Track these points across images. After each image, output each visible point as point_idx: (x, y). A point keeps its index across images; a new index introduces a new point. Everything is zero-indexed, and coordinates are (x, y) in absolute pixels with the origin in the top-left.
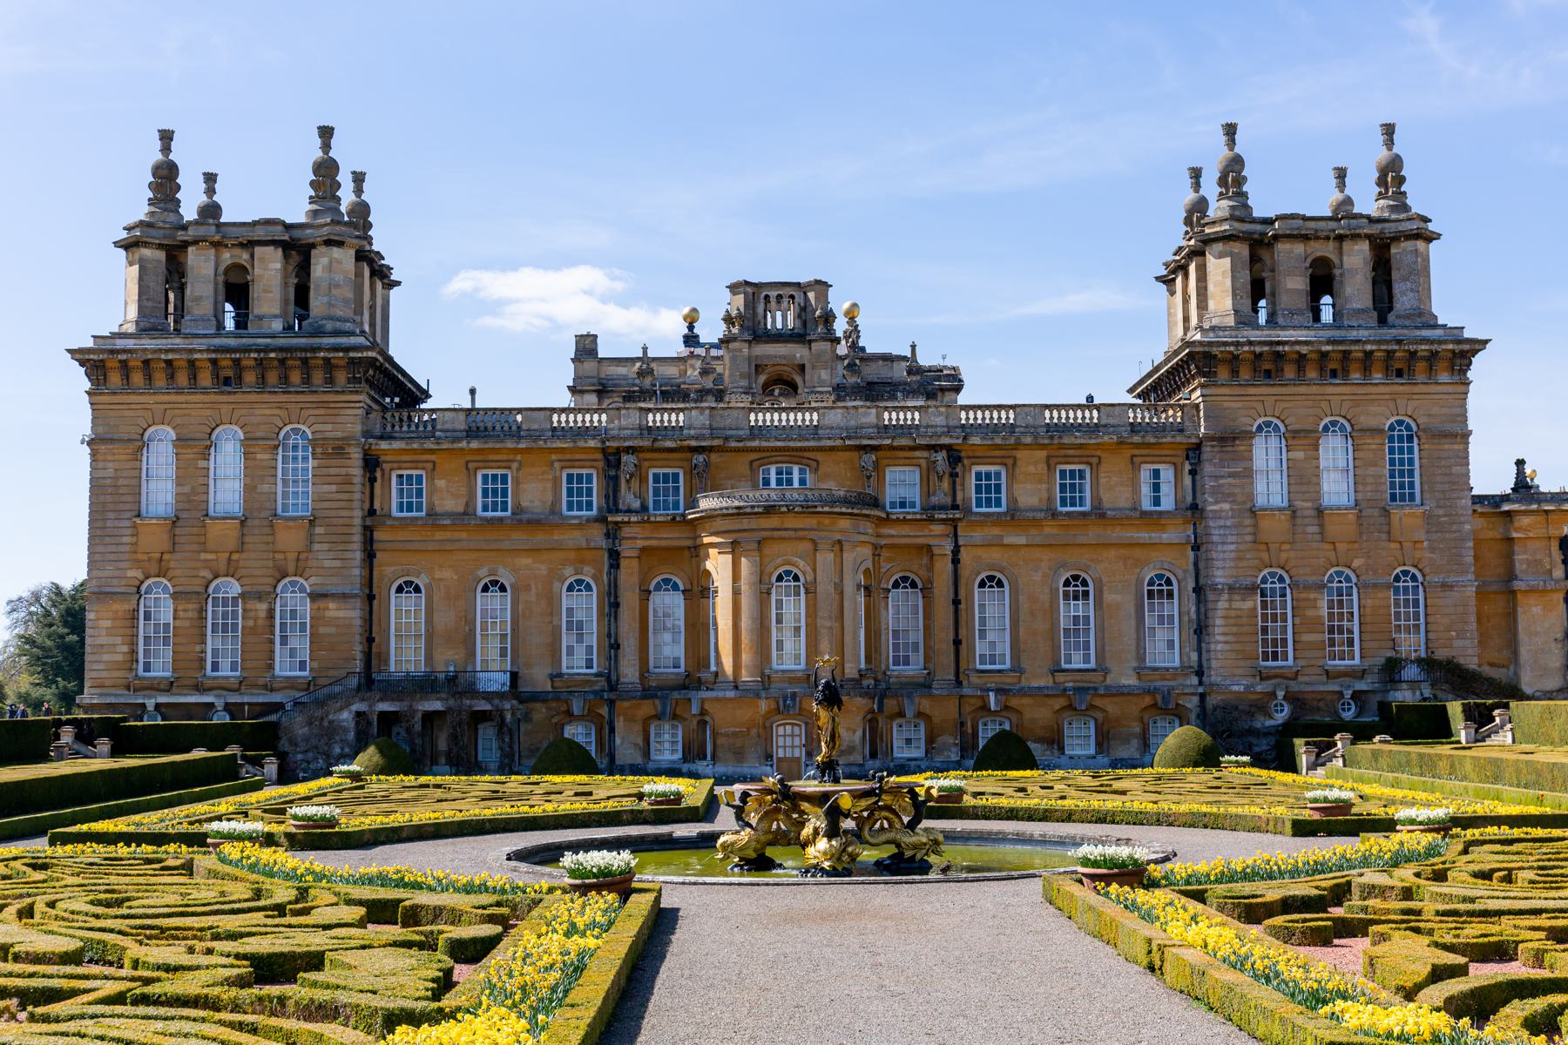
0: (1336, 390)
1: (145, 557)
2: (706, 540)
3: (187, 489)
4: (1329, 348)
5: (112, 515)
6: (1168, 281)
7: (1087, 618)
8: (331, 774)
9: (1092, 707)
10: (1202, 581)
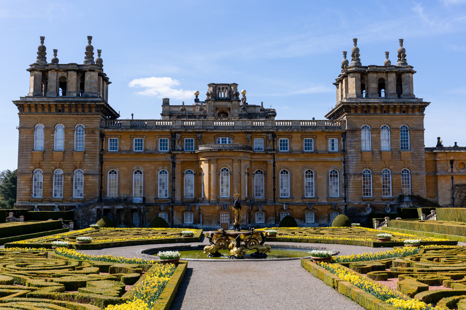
0: (386, 117)
1: (35, 162)
2: (201, 159)
3: (47, 143)
4: (384, 104)
5: (25, 150)
6: (336, 85)
7: (312, 183)
8: (89, 227)
9: (314, 209)
10: (346, 172)
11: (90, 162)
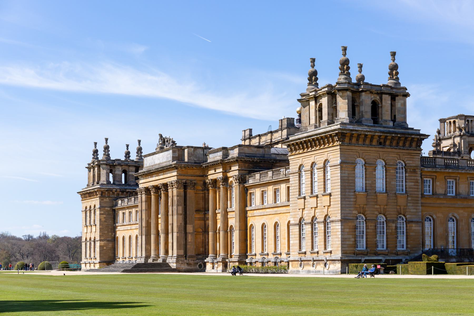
5: (347, 190)
11: (413, 208)
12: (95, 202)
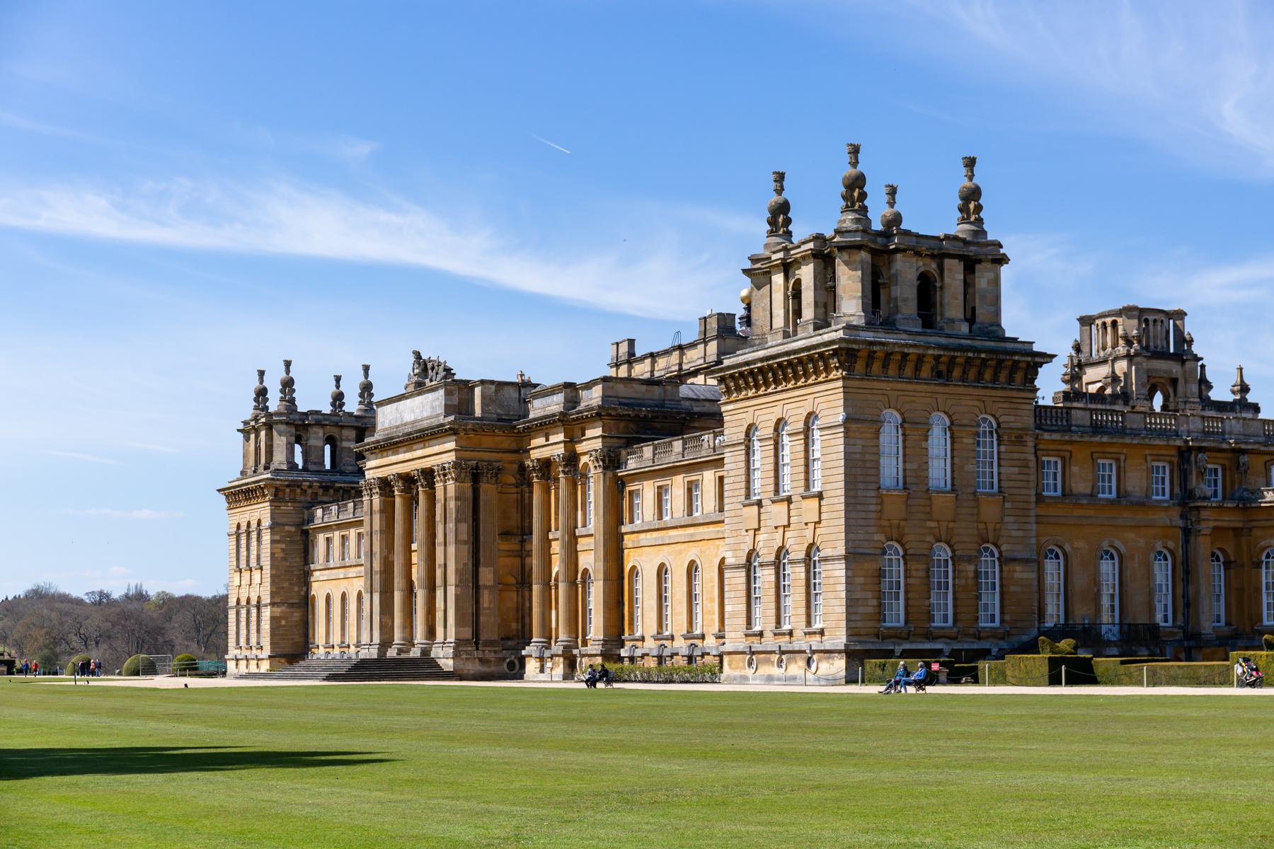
5: (861, 486)
12: (261, 512)
